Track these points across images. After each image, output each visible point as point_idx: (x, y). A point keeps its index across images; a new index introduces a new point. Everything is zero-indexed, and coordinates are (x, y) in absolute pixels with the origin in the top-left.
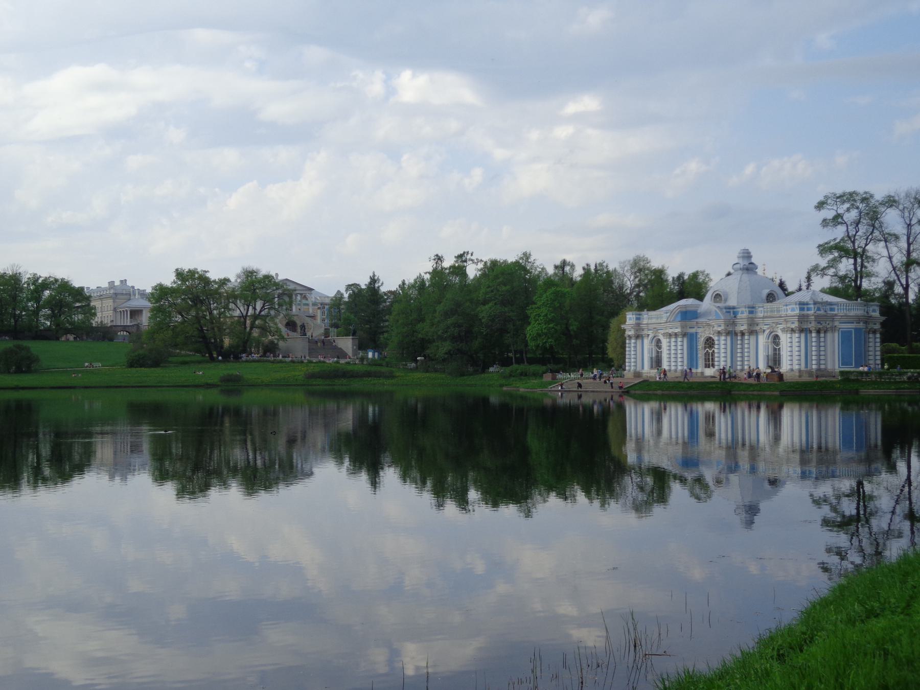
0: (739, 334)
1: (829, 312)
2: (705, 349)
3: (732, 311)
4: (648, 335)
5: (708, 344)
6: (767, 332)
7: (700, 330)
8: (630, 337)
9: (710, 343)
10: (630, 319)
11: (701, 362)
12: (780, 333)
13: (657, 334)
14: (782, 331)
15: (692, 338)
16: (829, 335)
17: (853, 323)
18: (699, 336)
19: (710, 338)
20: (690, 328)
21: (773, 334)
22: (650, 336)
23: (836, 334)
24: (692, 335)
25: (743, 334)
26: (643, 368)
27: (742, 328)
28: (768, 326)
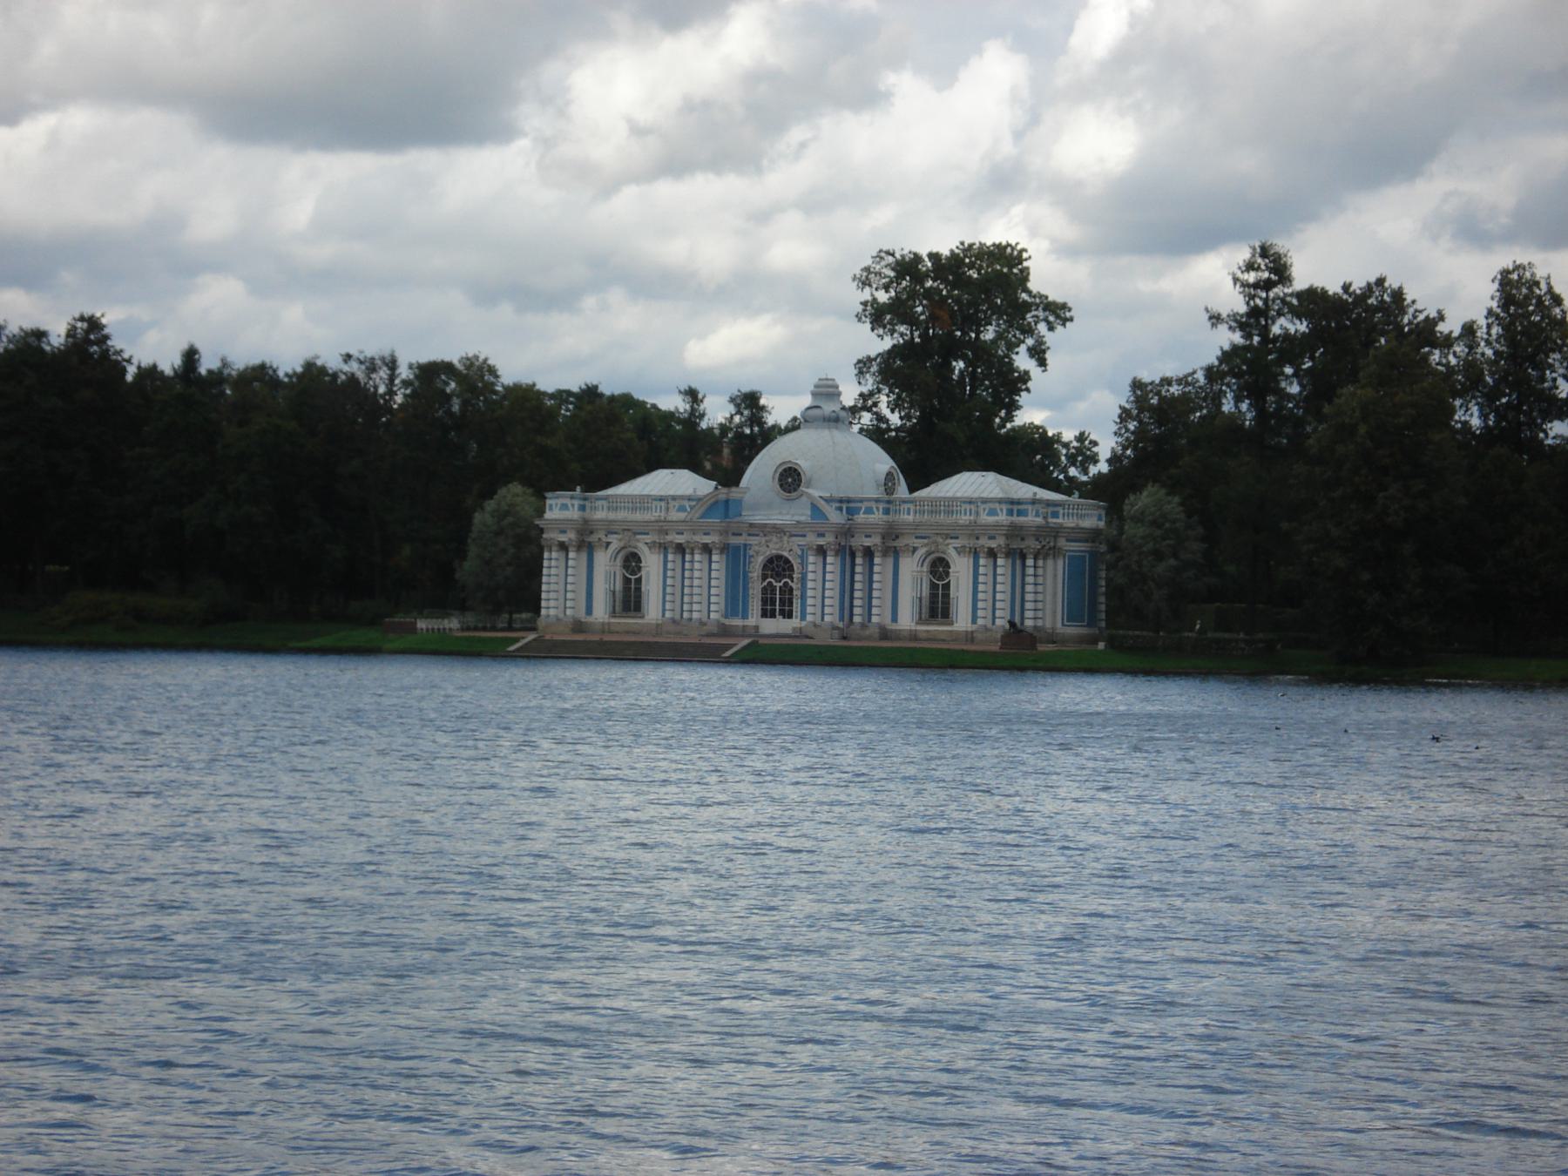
0: (859, 554)
1: (1050, 520)
2: (764, 580)
3: (844, 506)
4: (608, 544)
5: (773, 570)
6: (921, 552)
7: (753, 541)
8: (563, 547)
9: (778, 566)
10: (564, 507)
11: (755, 605)
12: (952, 555)
13: (633, 543)
14: (959, 553)
15: (736, 556)
16: (1050, 562)
17: (1087, 541)
18: (751, 553)
19: (780, 557)
20: (734, 534)
21: (933, 556)
22: (612, 548)
23: (1060, 563)
24: (737, 548)
25: (869, 553)
26: (589, 611)
27: (868, 542)
28: (926, 541)
